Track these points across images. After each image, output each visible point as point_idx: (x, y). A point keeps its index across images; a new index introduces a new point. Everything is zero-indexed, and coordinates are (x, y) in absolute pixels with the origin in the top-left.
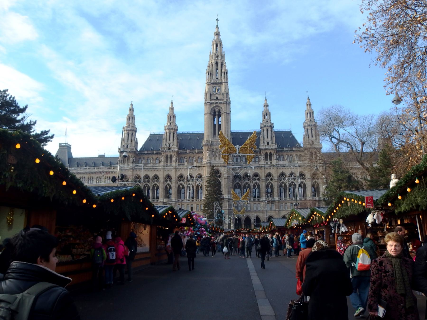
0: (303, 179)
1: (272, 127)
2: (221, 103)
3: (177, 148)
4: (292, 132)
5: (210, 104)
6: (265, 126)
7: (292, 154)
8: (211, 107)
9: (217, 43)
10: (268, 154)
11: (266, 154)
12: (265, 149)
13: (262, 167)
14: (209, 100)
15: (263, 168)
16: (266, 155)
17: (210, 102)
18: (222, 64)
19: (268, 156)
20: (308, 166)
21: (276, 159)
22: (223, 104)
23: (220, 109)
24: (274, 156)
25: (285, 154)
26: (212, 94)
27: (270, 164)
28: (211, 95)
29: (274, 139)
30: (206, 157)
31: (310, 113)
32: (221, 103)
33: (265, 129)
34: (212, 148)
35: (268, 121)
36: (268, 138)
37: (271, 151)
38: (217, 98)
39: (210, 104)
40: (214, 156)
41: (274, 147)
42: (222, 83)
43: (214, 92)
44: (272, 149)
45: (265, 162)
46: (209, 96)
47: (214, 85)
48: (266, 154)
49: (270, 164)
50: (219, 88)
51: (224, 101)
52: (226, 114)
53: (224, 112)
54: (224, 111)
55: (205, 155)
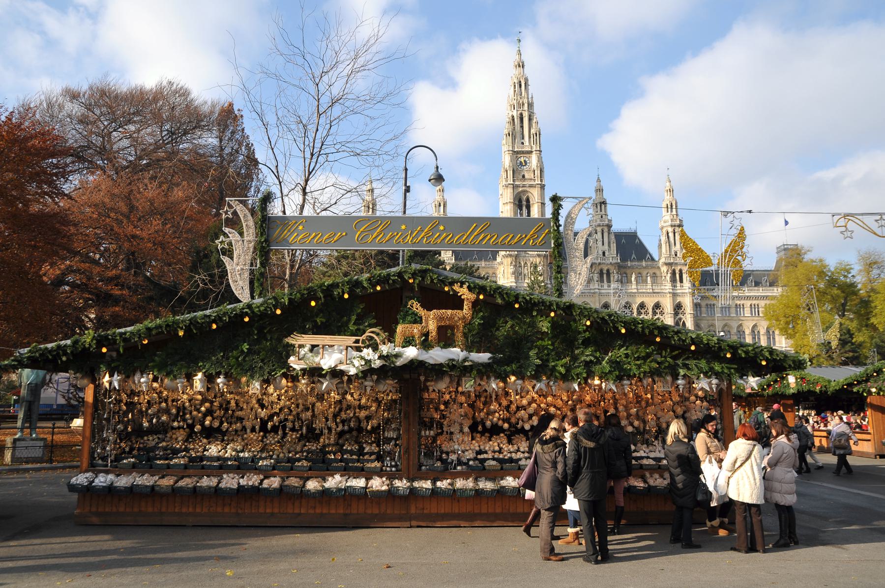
0: (660, 313)
1: (609, 226)
2: (531, 186)
3: (453, 258)
4: (638, 234)
5: (513, 187)
6: (599, 225)
7: (641, 271)
8: (515, 193)
9: (520, 82)
10: (605, 272)
11: (601, 270)
12: (600, 264)
13: (594, 293)
14: (512, 180)
15: (597, 295)
16: (601, 273)
17: (513, 184)
18: (530, 119)
19: (605, 276)
20: (670, 293)
21: (617, 281)
22: (535, 187)
23: (530, 195)
24: (615, 276)
25: (628, 271)
26: (515, 169)
27: (607, 288)
28: (513, 171)
29: (614, 246)
30: (510, 276)
31: (672, 204)
32: (531, 186)
33: (599, 229)
34: (518, 261)
35: (604, 216)
36: (603, 245)
37: (609, 266)
38: (524, 176)
39: (515, 187)
40: (521, 274)
41: (615, 261)
42: (531, 152)
43: (518, 166)
44: (611, 264)
45: (600, 285)
46: (510, 173)
47: (519, 156)
48: (601, 270)
49: (607, 288)
50: (527, 160)
51: (536, 182)
52: (540, 204)
53: (537, 201)
54: (536, 199)
55: (506, 271)
